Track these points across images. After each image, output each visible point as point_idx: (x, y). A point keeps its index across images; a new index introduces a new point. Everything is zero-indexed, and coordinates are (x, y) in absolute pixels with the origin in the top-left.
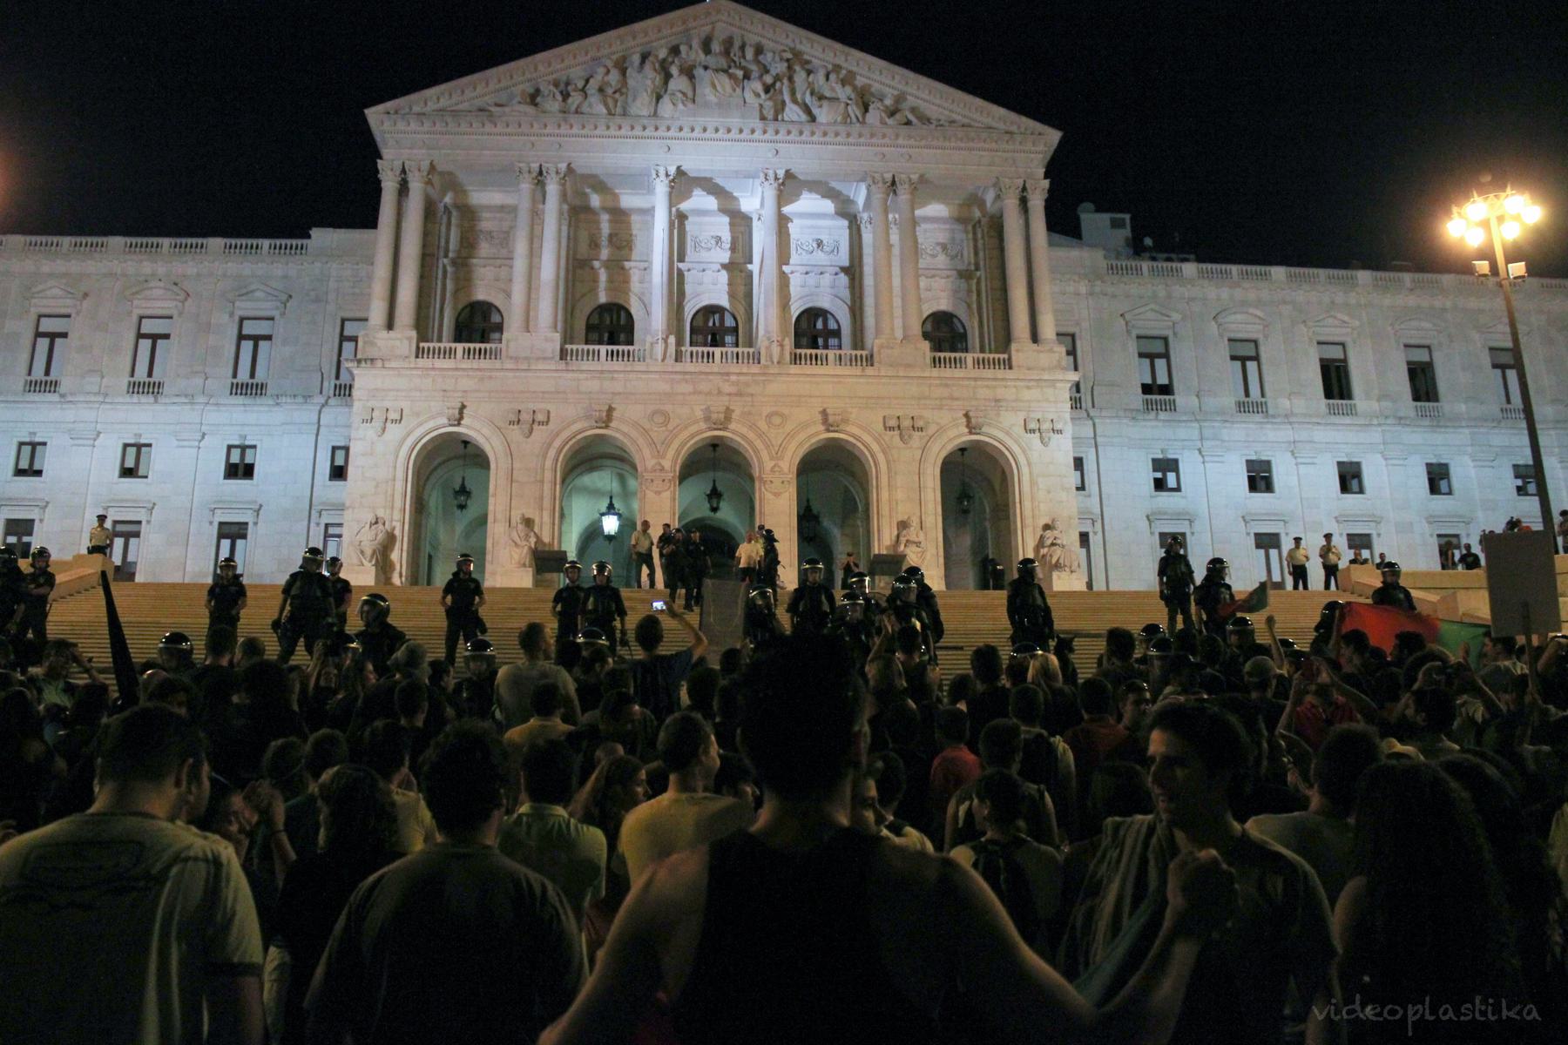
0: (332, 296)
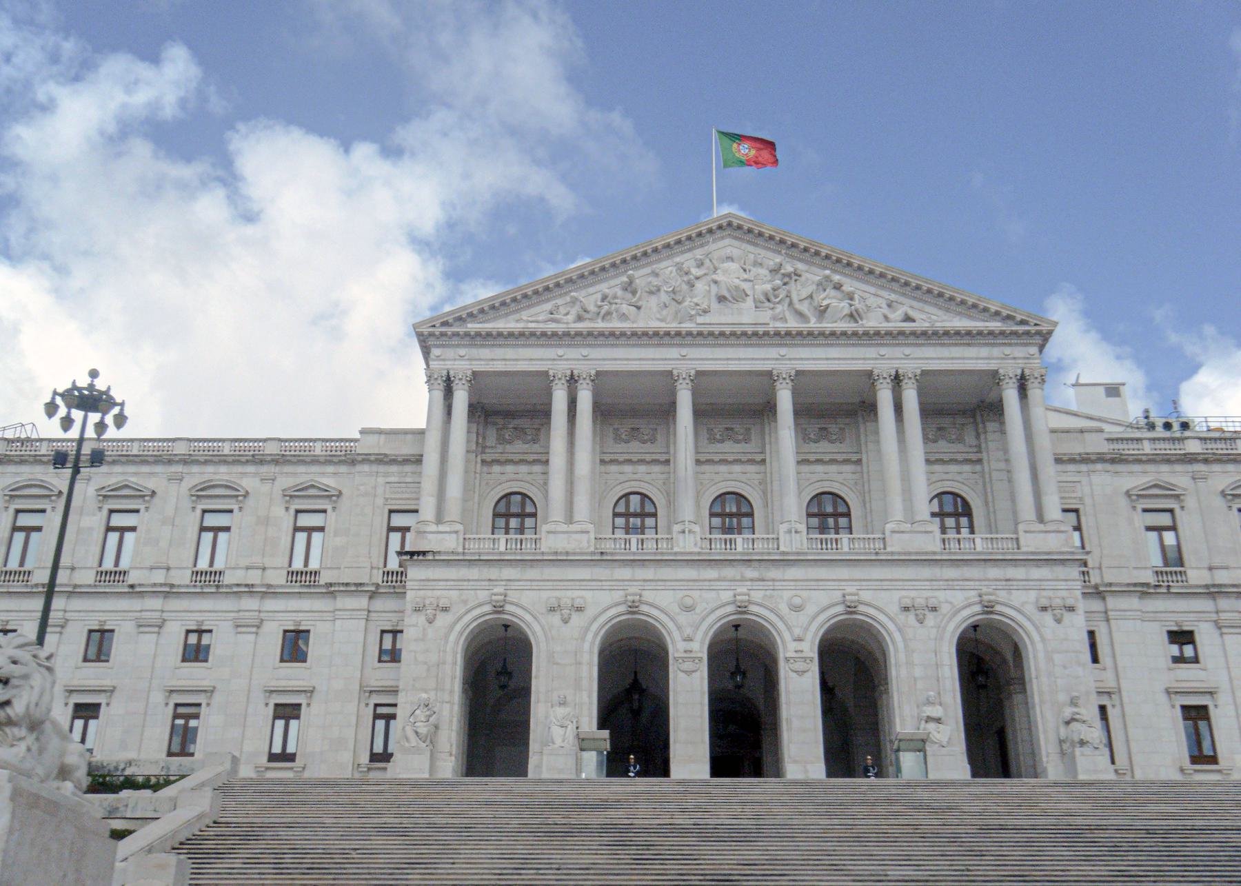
0: (380, 491)
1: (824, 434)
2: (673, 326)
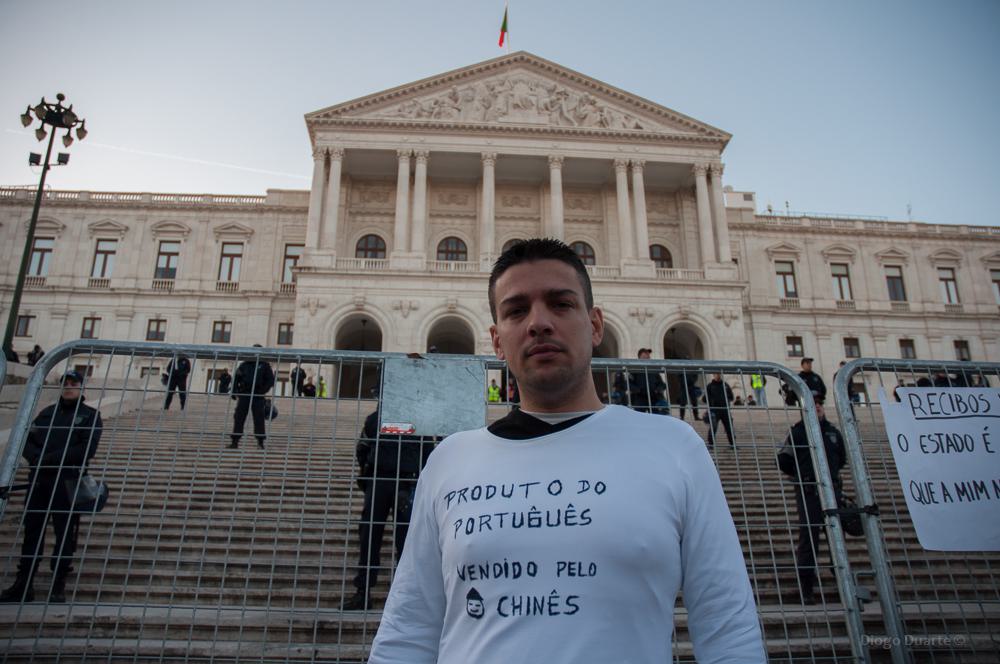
0: (279, 231)
1: (579, 204)
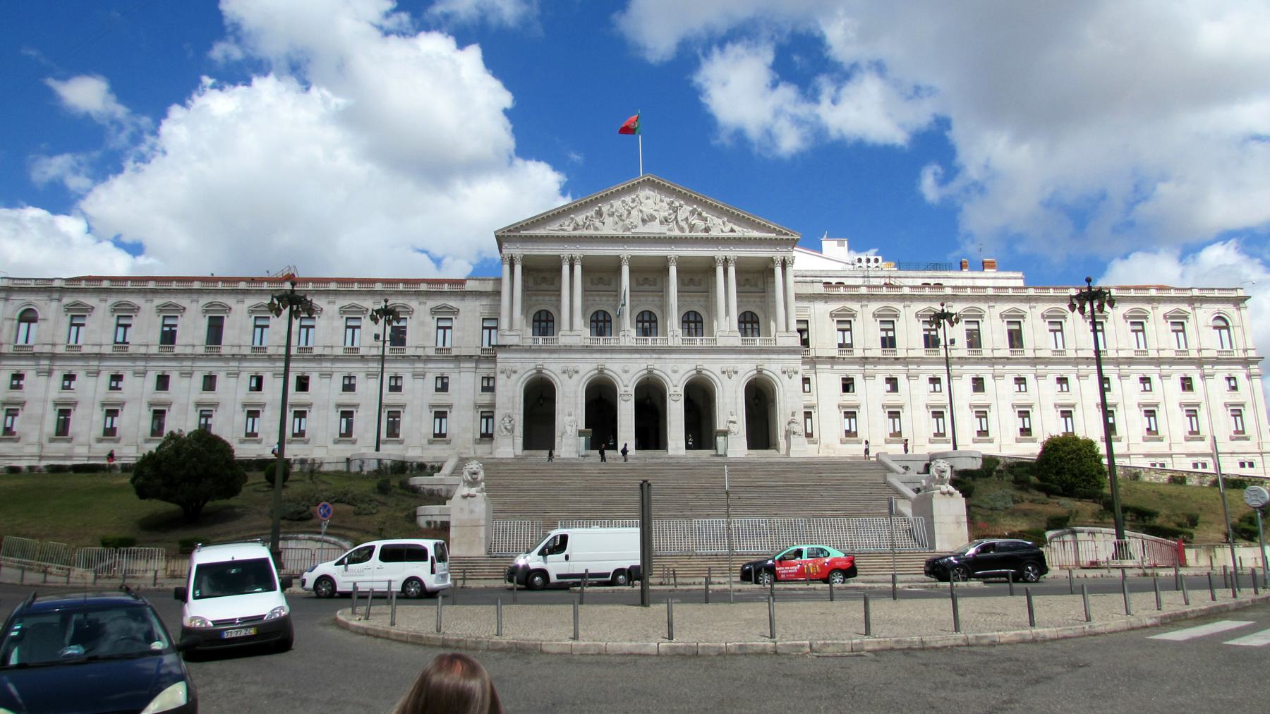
2: (620, 233)
